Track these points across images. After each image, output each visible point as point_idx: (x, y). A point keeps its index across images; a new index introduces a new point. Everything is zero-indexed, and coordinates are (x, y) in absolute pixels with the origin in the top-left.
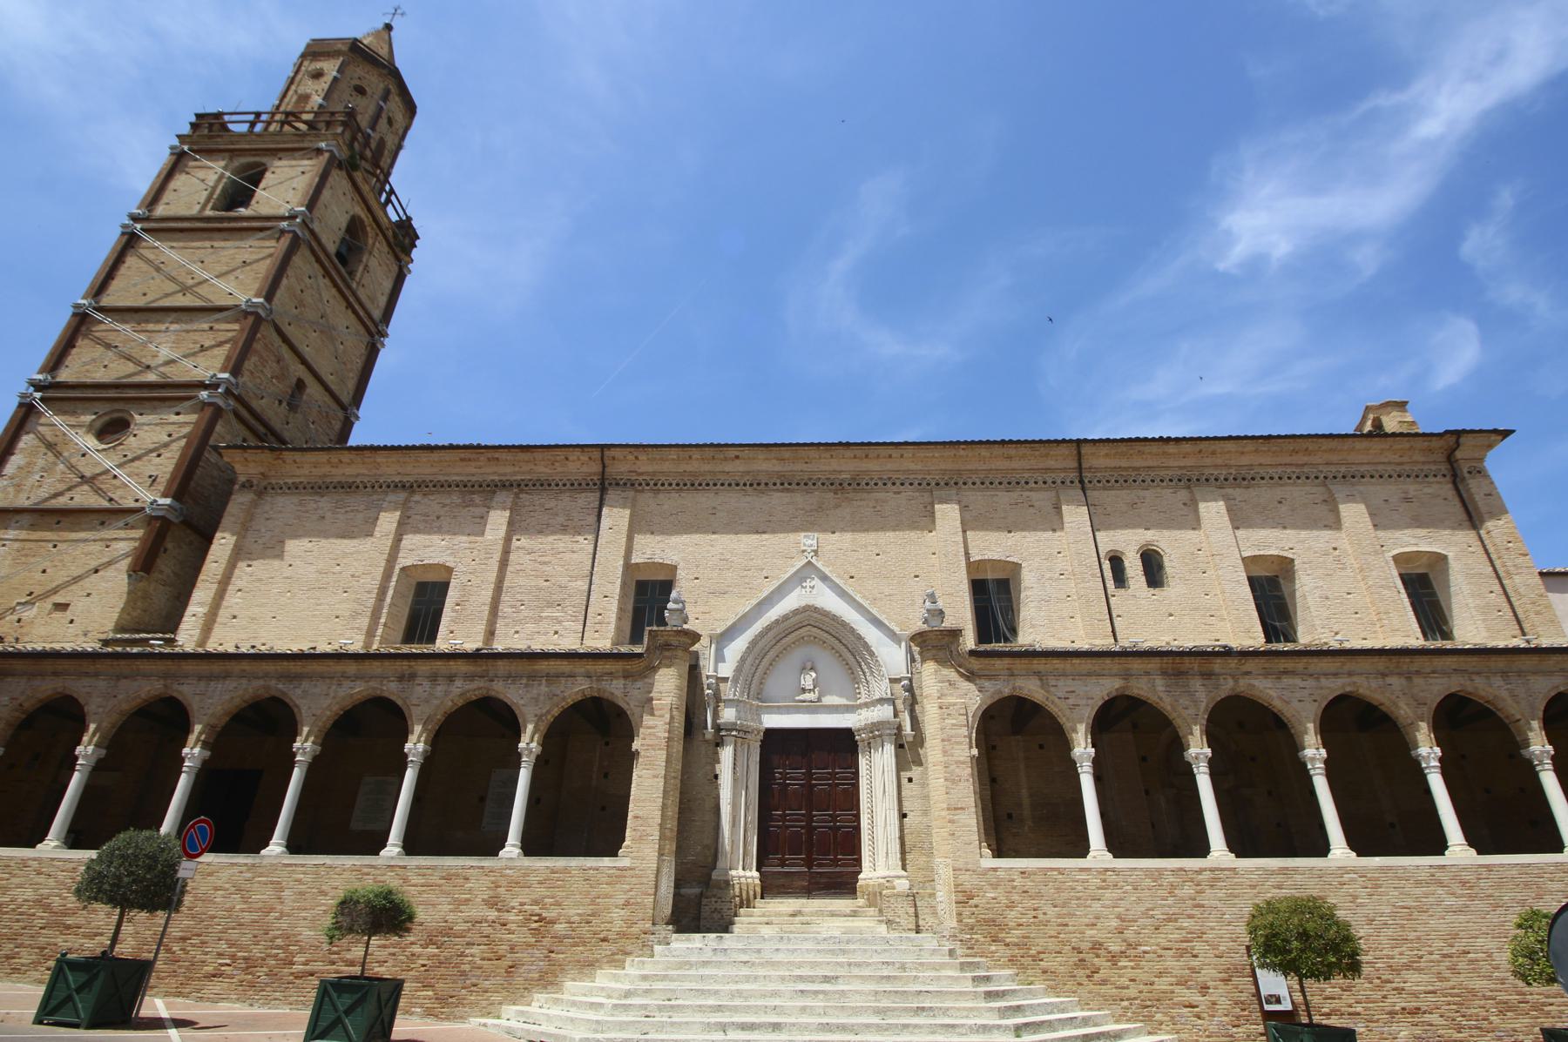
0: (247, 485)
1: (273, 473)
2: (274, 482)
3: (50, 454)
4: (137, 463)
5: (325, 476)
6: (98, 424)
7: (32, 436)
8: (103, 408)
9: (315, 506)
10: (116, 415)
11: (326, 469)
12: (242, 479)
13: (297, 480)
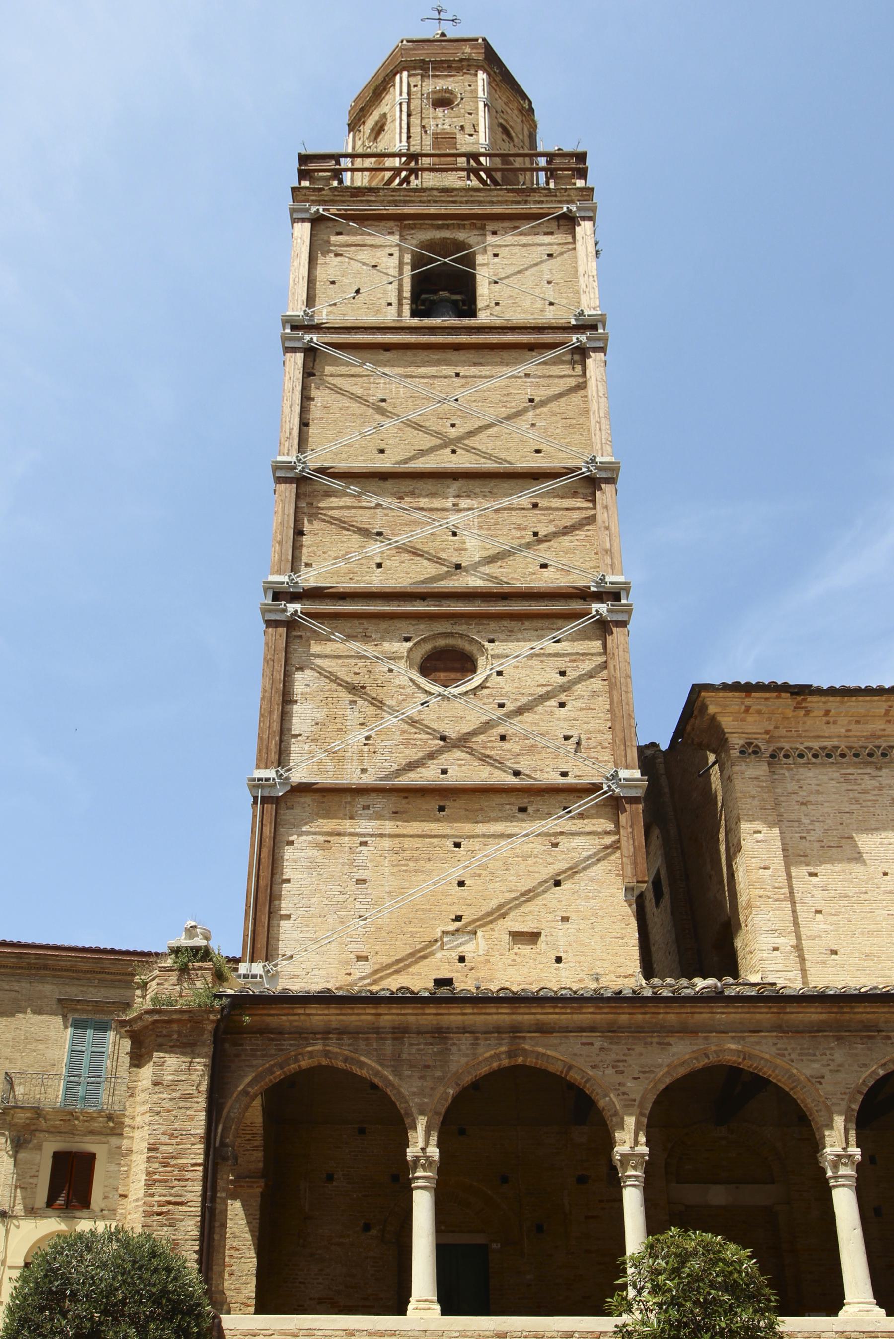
0: (750, 751)
1: (783, 732)
2: (787, 746)
3: (360, 702)
4: (528, 717)
5: (874, 736)
6: (418, 655)
7: (308, 672)
8: (423, 630)
9: (874, 783)
10: (441, 642)
11: (878, 725)
12: (736, 742)
13: (828, 743)
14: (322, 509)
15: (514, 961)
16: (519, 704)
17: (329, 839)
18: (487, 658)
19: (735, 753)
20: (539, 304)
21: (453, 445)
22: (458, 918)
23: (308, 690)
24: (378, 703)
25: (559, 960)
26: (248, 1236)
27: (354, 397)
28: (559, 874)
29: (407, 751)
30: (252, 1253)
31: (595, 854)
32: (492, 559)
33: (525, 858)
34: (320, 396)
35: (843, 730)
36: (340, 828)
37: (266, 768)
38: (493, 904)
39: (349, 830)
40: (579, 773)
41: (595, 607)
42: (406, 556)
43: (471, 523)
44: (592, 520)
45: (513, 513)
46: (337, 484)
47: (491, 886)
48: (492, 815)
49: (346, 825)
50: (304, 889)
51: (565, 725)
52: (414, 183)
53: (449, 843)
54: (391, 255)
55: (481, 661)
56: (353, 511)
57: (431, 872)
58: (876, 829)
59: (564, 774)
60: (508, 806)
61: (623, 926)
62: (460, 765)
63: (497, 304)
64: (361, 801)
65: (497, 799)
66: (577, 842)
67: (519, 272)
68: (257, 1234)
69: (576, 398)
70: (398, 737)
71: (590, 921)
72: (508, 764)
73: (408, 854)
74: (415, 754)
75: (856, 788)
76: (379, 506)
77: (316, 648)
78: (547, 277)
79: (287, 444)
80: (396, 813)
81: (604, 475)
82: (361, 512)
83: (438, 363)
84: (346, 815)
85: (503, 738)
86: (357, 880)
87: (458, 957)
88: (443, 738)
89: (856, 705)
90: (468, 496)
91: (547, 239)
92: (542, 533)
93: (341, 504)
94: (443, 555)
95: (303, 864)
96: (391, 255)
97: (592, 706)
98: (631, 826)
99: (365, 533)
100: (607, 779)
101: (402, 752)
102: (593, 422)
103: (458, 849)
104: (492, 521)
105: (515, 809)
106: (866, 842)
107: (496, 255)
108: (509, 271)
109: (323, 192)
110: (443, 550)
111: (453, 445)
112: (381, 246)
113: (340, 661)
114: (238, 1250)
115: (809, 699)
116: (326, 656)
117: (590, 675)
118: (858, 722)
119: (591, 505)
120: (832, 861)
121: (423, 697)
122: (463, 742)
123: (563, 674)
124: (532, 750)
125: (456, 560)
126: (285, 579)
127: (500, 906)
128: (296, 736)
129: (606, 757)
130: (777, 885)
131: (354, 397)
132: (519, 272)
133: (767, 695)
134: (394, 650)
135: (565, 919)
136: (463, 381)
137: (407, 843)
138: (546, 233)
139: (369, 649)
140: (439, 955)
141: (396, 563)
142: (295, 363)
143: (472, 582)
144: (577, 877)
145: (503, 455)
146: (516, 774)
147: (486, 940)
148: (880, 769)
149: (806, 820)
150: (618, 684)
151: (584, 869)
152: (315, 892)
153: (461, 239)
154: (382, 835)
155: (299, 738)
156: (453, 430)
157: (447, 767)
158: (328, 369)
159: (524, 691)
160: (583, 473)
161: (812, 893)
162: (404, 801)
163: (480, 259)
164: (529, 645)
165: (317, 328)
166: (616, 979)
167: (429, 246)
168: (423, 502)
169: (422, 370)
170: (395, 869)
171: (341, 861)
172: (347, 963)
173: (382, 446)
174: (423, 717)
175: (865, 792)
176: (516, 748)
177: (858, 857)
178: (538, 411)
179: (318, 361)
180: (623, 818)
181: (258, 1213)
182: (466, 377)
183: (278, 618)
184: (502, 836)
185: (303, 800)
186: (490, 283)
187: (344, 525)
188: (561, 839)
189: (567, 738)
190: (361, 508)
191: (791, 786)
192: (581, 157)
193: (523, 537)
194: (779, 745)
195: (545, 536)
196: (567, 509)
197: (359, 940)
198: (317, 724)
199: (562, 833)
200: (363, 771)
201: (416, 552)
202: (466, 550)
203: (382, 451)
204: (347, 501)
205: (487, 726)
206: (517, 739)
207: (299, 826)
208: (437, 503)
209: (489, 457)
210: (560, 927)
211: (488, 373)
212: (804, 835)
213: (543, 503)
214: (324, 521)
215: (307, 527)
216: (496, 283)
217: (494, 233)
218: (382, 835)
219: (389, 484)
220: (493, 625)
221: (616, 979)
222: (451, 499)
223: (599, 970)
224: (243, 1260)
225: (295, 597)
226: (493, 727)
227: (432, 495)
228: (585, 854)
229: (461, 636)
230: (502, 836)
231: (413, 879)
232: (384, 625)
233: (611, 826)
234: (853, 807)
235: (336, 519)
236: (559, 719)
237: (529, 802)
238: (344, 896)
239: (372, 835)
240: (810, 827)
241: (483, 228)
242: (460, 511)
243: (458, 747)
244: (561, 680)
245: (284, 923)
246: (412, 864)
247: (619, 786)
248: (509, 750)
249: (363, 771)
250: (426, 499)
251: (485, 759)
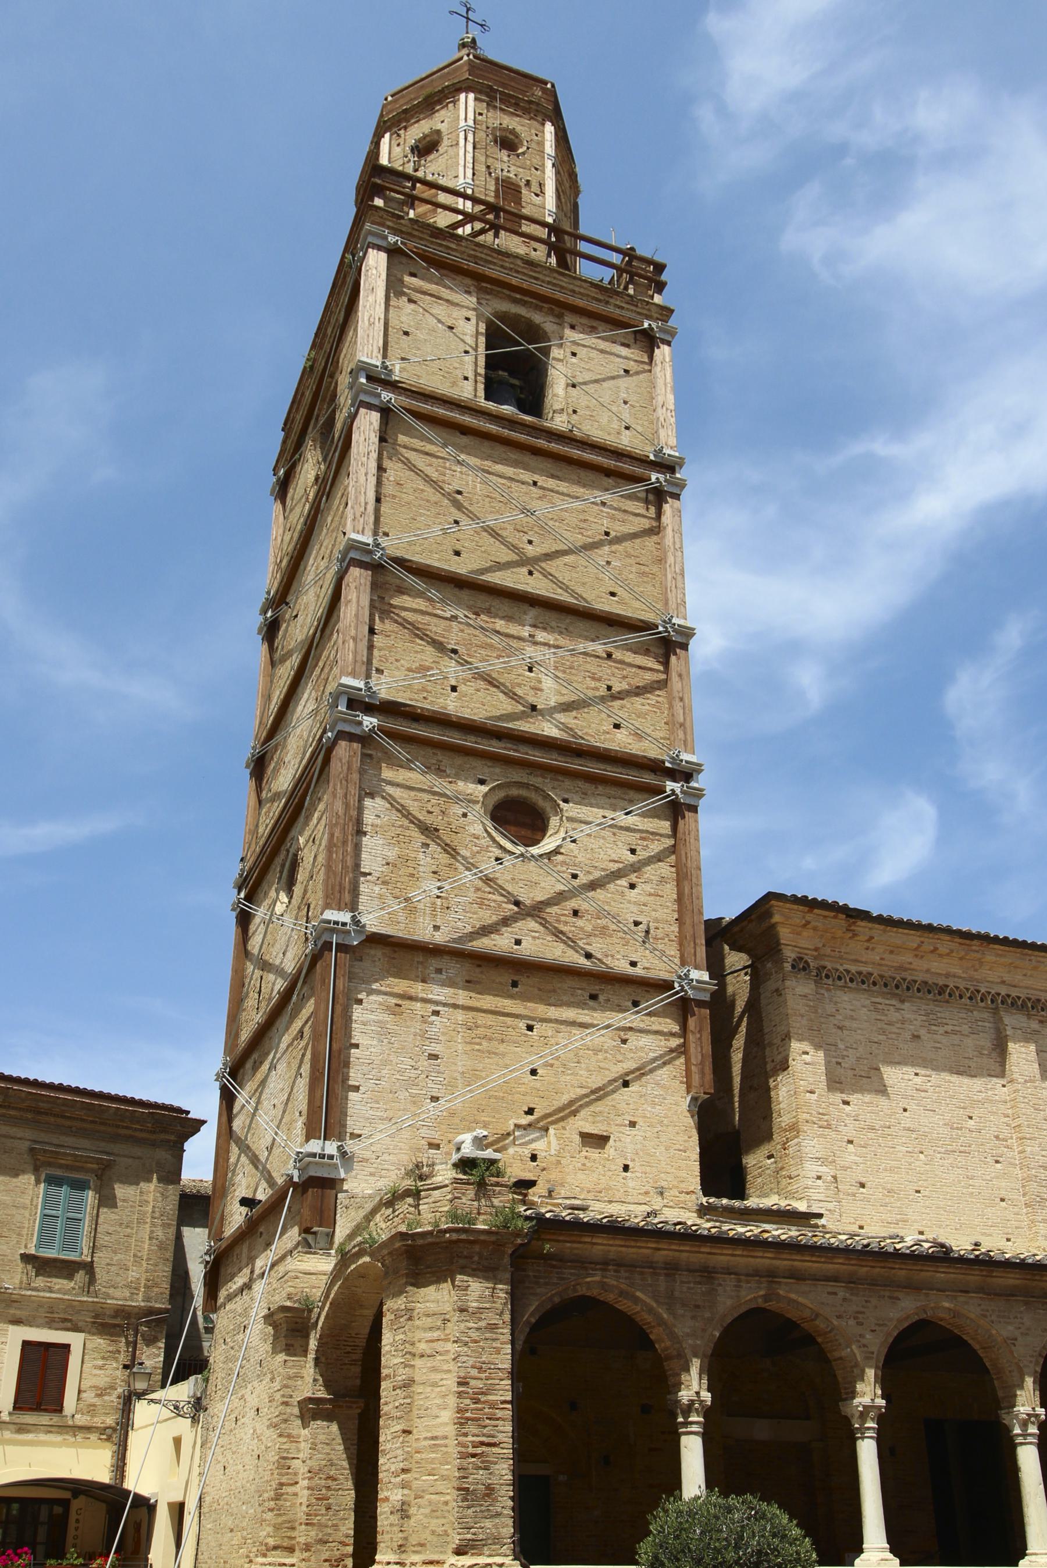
0: (801, 966)
1: (828, 951)
3: (433, 847)
4: (599, 894)
5: (901, 968)
8: (498, 776)
10: (515, 792)
11: (906, 958)
12: (789, 954)
14: (395, 607)
15: (584, 1165)
16: (591, 878)
17: (400, 1002)
18: (561, 819)
19: (788, 967)
20: (615, 425)
21: (530, 564)
22: (530, 1111)
23: (378, 822)
24: (451, 851)
25: (626, 1168)
26: (345, 1464)
27: (428, 480)
28: (627, 1074)
29: (481, 913)
30: (350, 1484)
31: (661, 1056)
32: (567, 707)
33: (596, 1051)
34: (394, 470)
35: (878, 958)
36: (412, 992)
37: (339, 910)
38: (565, 1099)
39: (420, 995)
40: (647, 965)
41: (670, 785)
42: (482, 684)
43: (547, 661)
44: (663, 684)
45: (589, 659)
46: (411, 580)
47: (563, 1078)
48: (565, 998)
49: (418, 989)
50: (374, 1058)
51: (635, 909)
52: (488, 238)
53: (522, 1025)
54: (468, 319)
55: (554, 821)
56: (427, 618)
57: (503, 1055)
58: (899, 1063)
59: (633, 964)
60: (580, 992)
61: (686, 1138)
62: (534, 938)
63: (575, 412)
64: (434, 963)
65: (570, 982)
66: (645, 1041)
67: (596, 381)
68: (355, 1462)
69: (650, 542)
70: (472, 895)
71: (656, 1130)
72: (581, 943)
73: (481, 1031)
74: (489, 917)
75: (883, 1018)
76: (454, 618)
77: (387, 773)
78: (623, 395)
79: (362, 520)
80: (468, 982)
81: (679, 639)
82: (435, 620)
83: (515, 464)
84: (418, 977)
85: (576, 913)
86: (429, 1054)
87: (530, 1155)
88: (517, 903)
89: (896, 937)
90: (545, 629)
91: (624, 351)
92: (616, 688)
93: (415, 606)
94: (519, 692)
95: (373, 1028)
96: (468, 319)
97: (660, 893)
98: (700, 1032)
99: (439, 646)
100: (680, 977)
101: (474, 913)
102: (669, 577)
103: (530, 1033)
104: (568, 663)
105: (587, 995)
106: (893, 1075)
107: (574, 354)
108: (588, 377)
109: (402, 221)
110: (519, 685)
111: (530, 564)
112: (457, 305)
113: (413, 793)
114: (335, 1480)
115: (860, 923)
116: (398, 785)
117: (658, 858)
118: (891, 952)
119: (661, 668)
120: (862, 1090)
121: (498, 852)
122: (536, 911)
123: (633, 851)
124: (603, 931)
125: (532, 700)
126: (360, 684)
127: (571, 1103)
128: (366, 874)
129: (673, 951)
130: (821, 1111)
131: (428, 480)
132: (596, 381)
133: (827, 913)
134: (469, 791)
135: (633, 1124)
136: (541, 492)
137: (482, 1019)
138: (623, 345)
139: (440, 784)
140: (511, 1151)
141: (471, 691)
142: (371, 424)
143: (549, 729)
144: (644, 1079)
145: (580, 590)
146: (588, 956)
147: (559, 1139)
148: (902, 1001)
149: (841, 1046)
150: (689, 873)
151: (651, 1071)
152: (385, 1063)
153: (537, 322)
154: (455, 1006)
155: (369, 877)
156: (530, 547)
157: (521, 937)
158: (402, 439)
159: (597, 864)
160: (660, 633)
161: (846, 1121)
162: (478, 970)
163: (555, 352)
164: (601, 812)
165: (393, 386)
166: (678, 1195)
167: (503, 317)
168: (500, 624)
169: (499, 468)
170: (469, 1047)
171: (413, 1030)
172: (419, 1150)
173: (458, 547)
174: (498, 875)
175: (890, 1024)
176: (589, 928)
177: (882, 1090)
178: (614, 547)
179: (390, 425)
180: (692, 1022)
181: (356, 1437)
182: (543, 488)
183: (353, 731)
184: (573, 1024)
185: (373, 952)
186: (568, 385)
187: (418, 632)
188: (630, 1035)
189: (637, 924)
190: (436, 615)
191: (830, 1009)
192: (660, 268)
193: (597, 689)
194: (822, 963)
195: (619, 693)
196: (640, 667)
197: (431, 1124)
198: (388, 864)
199: (631, 1029)
200: (436, 928)
201: (491, 682)
202: (541, 690)
203: (457, 553)
204: (420, 604)
205: (559, 898)
206: (590, 916)
207: (369, 983)
208: (513, 629)
209: (566, 589)
210: (628, 1133)
211: (565, 490)
212: (840, 1060)
213: (617, 655)
214: (396, 622)
215: (378, 626)
216: (574, 386)
217: (573, 327)
218: (455, 1006)
219: (465, 595)
220: (568, 783)
221: (678, 1195)
222: (527, 628)
223: (664, 1184)
224: (340, 1492)
225: (369, 709)
226: (566, 899)
227: (509, 618)
228: (652, 1055)
229: (537, 789)
230: (573, 1024)
231: (487, 1060)
232: (459, 760)
233: (676, 1028)
234: (881, 1037)
235: (410, 623)
236: (629, 902)
237: (600, 990)
238: (416, 1072)
239: (445, 1005)
240: (845, 1053)
241: (560, 316)
242: (536, 643)
243: (532, 916)
244: (632, 858)
245: (352, 1095)
246: (485, 1043)
247: (693, 988)
248: (582, 929)
249: (436, 928)
250: (502, 622)
251: (558, 934)
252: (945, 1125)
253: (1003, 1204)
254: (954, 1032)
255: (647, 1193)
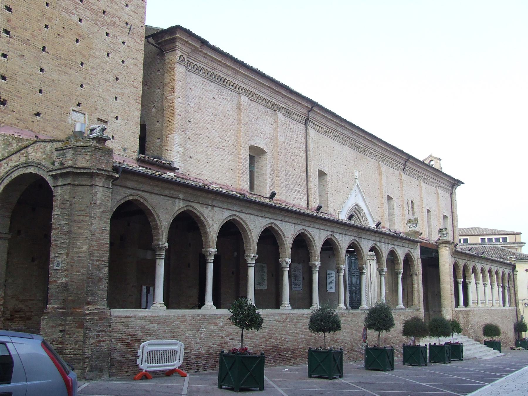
40: (129, 45)
51: (126, 16)
62: (87, 20)
71: (125, 122)
97: (137, 12)
103: (82, 67)
124: (114, 24)
147: (89, 119)
161: (189, 130)
166: (130, 152)
221: (130, 152)
223: (126, 147)
234: (204, 96)
236: (125, 13)
240: (191, 100)
246: (63, 67)
252: (218, 137)
253: (232, 171)
254: (226, 99)
255: (119, 150)
